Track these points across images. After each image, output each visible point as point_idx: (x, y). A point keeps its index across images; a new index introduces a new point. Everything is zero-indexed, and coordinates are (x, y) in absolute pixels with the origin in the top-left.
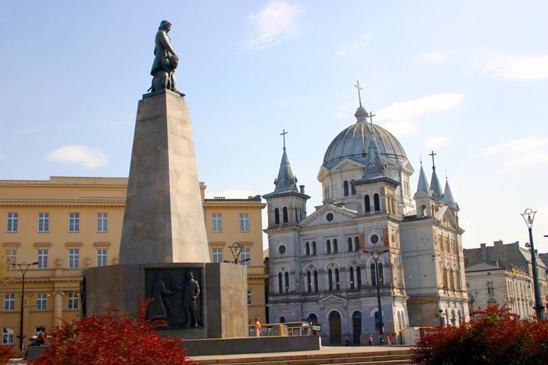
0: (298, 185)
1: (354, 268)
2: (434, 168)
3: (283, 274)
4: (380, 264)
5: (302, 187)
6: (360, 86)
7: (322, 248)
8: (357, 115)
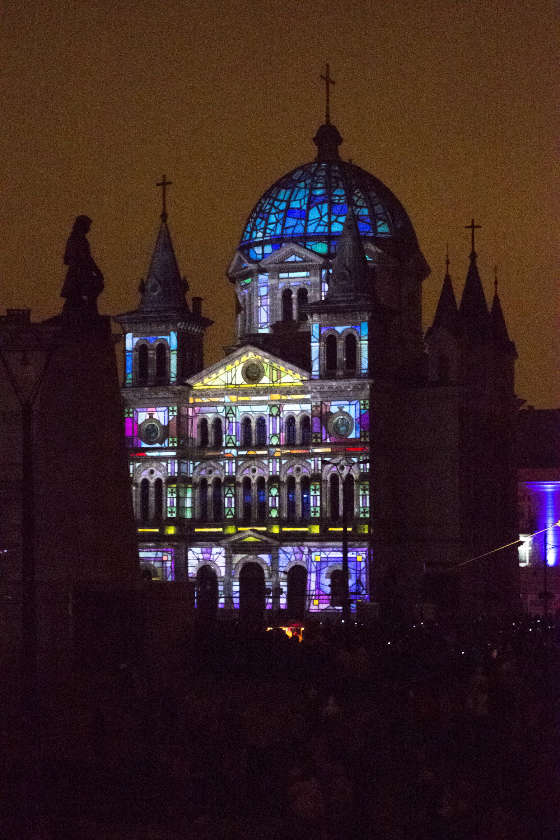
0: (189, 297)
1: (298, 480)
2: (473, 256)
3: (152, 482)
4: (349, 476)
5: (197, 301)
6: (332, 77)
7: (232, 434)
8: (318, 140)
